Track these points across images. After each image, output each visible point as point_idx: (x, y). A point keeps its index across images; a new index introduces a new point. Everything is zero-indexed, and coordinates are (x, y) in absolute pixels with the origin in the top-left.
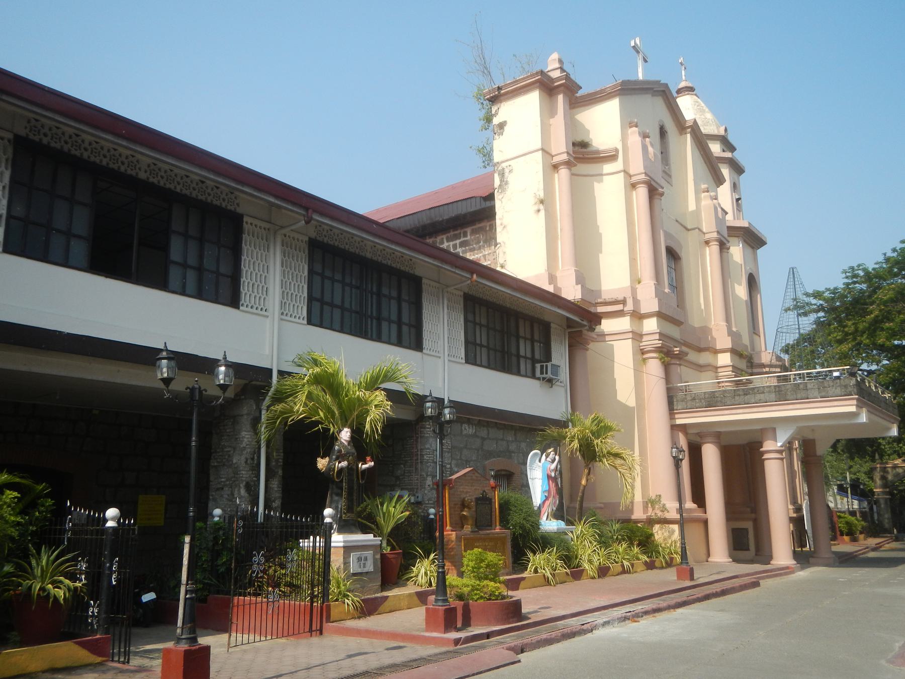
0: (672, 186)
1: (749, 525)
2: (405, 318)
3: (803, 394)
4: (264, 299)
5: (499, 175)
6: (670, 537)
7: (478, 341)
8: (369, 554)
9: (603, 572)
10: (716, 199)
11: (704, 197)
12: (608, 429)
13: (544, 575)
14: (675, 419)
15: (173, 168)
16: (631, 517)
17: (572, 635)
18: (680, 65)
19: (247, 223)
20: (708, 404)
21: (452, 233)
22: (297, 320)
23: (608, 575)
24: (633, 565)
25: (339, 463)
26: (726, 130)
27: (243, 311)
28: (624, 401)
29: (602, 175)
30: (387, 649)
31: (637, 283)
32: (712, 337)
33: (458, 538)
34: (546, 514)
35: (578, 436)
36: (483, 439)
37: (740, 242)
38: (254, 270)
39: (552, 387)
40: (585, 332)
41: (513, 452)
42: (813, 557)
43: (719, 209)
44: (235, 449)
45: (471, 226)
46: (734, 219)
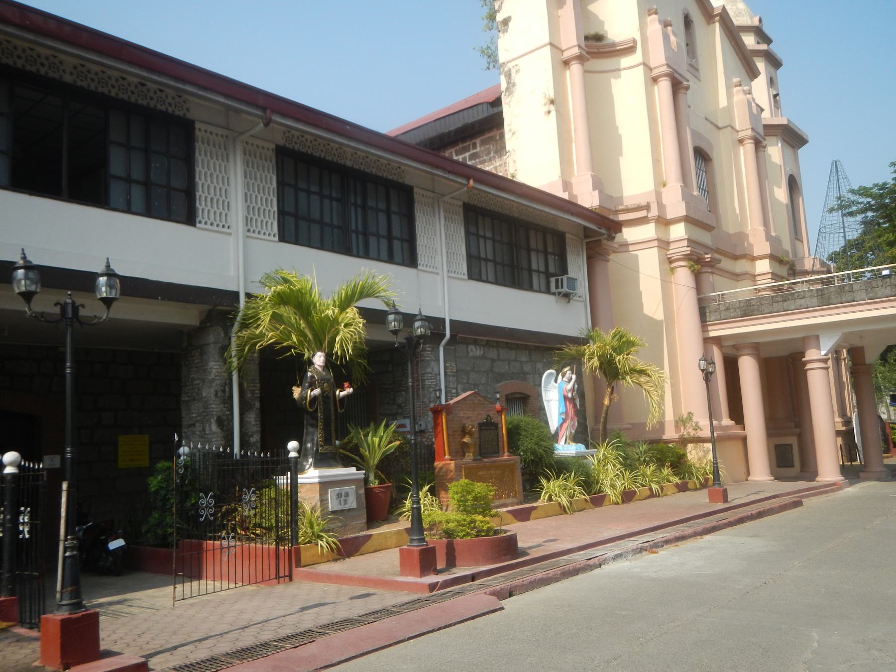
0: (700, 80)
1: (793, 441)
2: (396, 231)
3: (849, 297)
4: (226, 215)
5: (505, 76)
6: (705, 457)
7: (483, 255)
8: (351, 489)
9: (628, 496)
10: (750, 93)
11: (737, 92)
12: (631, 344)
13: (559, 504)
14: (708, 331)
15: (104, 69)
16: (662, 437)
17: (575, 572)
19: (200, 130)
20: (744, 314)
21: (461, 146)
22: (266, 237)
23: (634, 499)
24: (662, 488)
25: (312, 390)
26: (760, 20)
27: (200, 228)
28: (650, 314)
29: (619, 70)
30: (352, 598)
31: (662, 186)
32: (749, 244)
33: (458, 468)
34: (564, 438)
35: (597, 353)
36: (493, 361)
37: (779, 141)
38: (212, 183)
39: (569, 302)
40: (605, 242)
41: (528, 373)
42: (863, 472)
43: (753, 105)
44: (203, 381)
45: (480, 136)
46: (772, 116)
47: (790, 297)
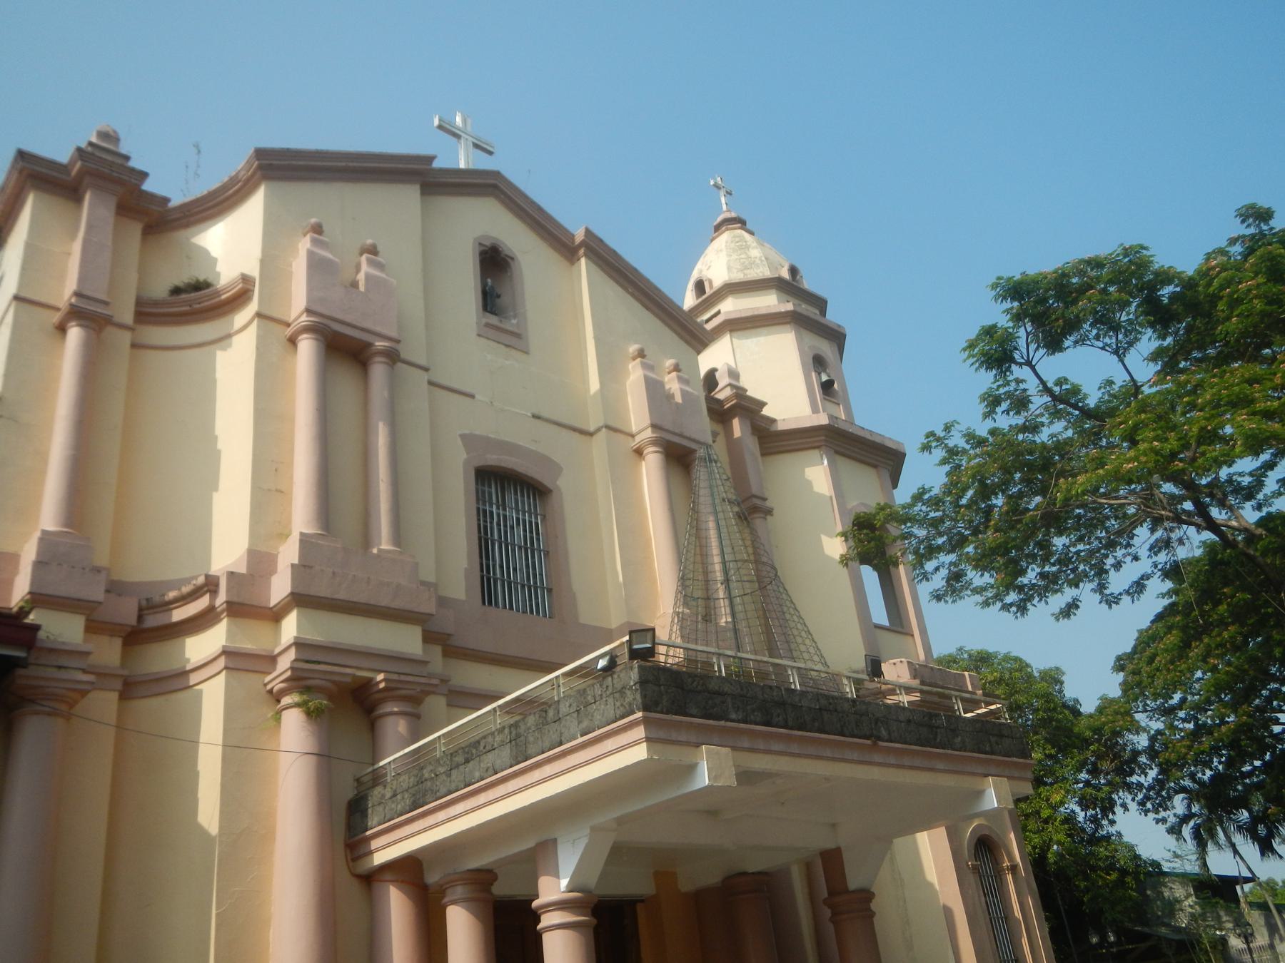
14: (371, 853)
18: (715, 189)
20: (414, 802)
26: (793, 271)
29: (229, 336)
37: (824, 456)
47: (474, 751)
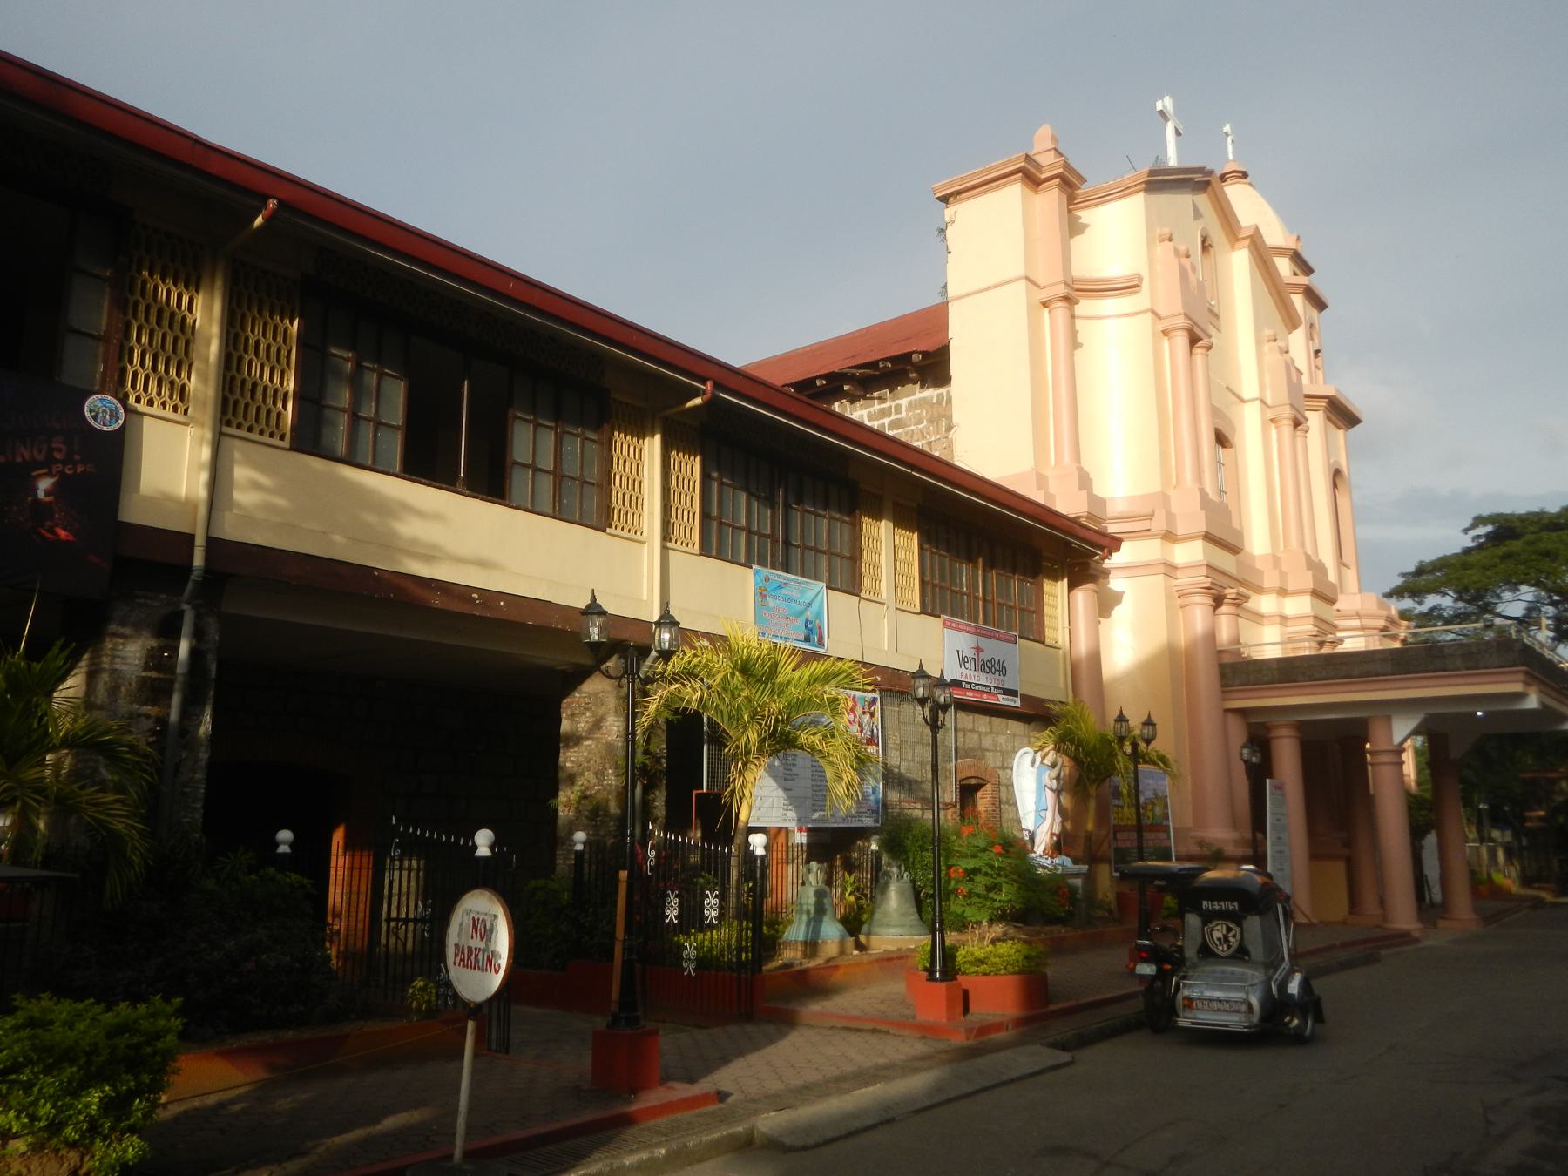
0: (1220, 332)
10: (1287, 352)
27: (610, 534)
41: (987, 750)
42: (1442, 918)
43: (1293, 371)
46: (1311, 382)
